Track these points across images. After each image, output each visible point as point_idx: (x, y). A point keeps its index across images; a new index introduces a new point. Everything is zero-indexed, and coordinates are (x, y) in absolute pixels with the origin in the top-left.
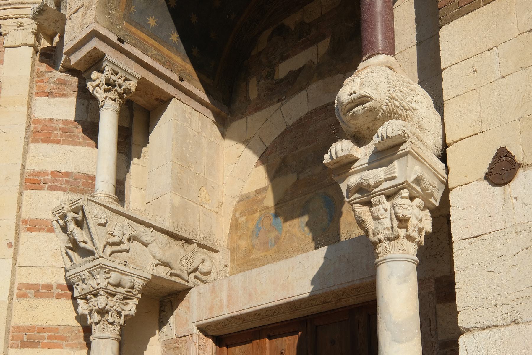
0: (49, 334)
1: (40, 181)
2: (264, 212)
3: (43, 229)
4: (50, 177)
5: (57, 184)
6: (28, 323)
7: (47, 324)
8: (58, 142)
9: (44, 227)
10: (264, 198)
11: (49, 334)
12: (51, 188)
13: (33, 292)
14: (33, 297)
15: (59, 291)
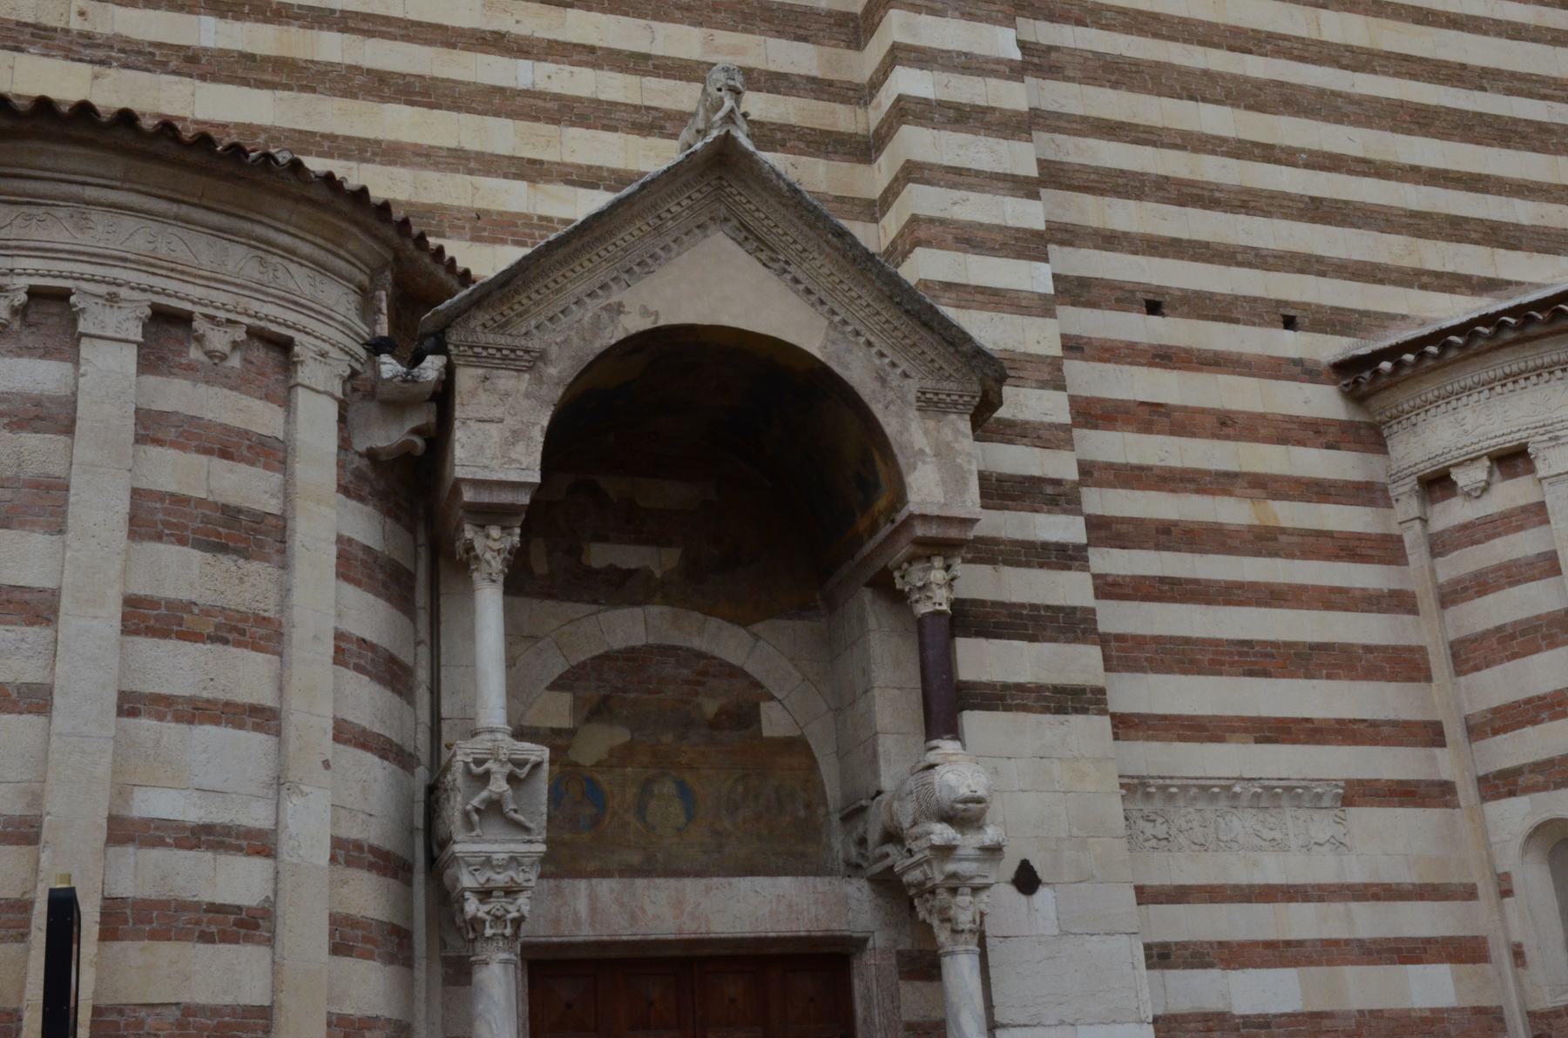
0: (364, 932)
1: (344, 650)
2: (568, 769)
3: (350, 741)
4: (354, 648)
5: (362, 662)
6: (340, 910)
7: (359, 916)
8: (358, 583)
9: (351, 737)
10: (568, 747)
11: (364, 932)
12: (359, 669)
13: (342, 852)
14: (342, 862)
15: (371, 858)
